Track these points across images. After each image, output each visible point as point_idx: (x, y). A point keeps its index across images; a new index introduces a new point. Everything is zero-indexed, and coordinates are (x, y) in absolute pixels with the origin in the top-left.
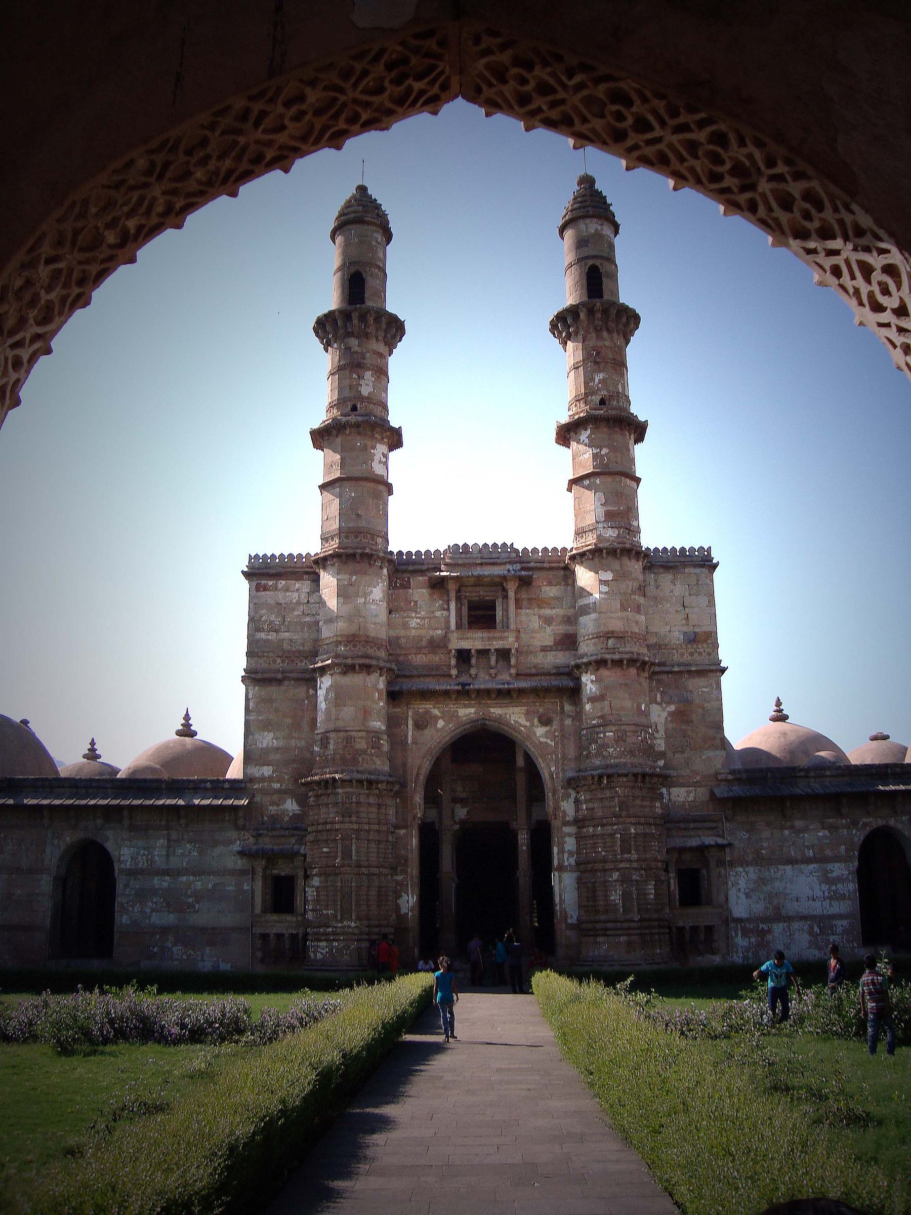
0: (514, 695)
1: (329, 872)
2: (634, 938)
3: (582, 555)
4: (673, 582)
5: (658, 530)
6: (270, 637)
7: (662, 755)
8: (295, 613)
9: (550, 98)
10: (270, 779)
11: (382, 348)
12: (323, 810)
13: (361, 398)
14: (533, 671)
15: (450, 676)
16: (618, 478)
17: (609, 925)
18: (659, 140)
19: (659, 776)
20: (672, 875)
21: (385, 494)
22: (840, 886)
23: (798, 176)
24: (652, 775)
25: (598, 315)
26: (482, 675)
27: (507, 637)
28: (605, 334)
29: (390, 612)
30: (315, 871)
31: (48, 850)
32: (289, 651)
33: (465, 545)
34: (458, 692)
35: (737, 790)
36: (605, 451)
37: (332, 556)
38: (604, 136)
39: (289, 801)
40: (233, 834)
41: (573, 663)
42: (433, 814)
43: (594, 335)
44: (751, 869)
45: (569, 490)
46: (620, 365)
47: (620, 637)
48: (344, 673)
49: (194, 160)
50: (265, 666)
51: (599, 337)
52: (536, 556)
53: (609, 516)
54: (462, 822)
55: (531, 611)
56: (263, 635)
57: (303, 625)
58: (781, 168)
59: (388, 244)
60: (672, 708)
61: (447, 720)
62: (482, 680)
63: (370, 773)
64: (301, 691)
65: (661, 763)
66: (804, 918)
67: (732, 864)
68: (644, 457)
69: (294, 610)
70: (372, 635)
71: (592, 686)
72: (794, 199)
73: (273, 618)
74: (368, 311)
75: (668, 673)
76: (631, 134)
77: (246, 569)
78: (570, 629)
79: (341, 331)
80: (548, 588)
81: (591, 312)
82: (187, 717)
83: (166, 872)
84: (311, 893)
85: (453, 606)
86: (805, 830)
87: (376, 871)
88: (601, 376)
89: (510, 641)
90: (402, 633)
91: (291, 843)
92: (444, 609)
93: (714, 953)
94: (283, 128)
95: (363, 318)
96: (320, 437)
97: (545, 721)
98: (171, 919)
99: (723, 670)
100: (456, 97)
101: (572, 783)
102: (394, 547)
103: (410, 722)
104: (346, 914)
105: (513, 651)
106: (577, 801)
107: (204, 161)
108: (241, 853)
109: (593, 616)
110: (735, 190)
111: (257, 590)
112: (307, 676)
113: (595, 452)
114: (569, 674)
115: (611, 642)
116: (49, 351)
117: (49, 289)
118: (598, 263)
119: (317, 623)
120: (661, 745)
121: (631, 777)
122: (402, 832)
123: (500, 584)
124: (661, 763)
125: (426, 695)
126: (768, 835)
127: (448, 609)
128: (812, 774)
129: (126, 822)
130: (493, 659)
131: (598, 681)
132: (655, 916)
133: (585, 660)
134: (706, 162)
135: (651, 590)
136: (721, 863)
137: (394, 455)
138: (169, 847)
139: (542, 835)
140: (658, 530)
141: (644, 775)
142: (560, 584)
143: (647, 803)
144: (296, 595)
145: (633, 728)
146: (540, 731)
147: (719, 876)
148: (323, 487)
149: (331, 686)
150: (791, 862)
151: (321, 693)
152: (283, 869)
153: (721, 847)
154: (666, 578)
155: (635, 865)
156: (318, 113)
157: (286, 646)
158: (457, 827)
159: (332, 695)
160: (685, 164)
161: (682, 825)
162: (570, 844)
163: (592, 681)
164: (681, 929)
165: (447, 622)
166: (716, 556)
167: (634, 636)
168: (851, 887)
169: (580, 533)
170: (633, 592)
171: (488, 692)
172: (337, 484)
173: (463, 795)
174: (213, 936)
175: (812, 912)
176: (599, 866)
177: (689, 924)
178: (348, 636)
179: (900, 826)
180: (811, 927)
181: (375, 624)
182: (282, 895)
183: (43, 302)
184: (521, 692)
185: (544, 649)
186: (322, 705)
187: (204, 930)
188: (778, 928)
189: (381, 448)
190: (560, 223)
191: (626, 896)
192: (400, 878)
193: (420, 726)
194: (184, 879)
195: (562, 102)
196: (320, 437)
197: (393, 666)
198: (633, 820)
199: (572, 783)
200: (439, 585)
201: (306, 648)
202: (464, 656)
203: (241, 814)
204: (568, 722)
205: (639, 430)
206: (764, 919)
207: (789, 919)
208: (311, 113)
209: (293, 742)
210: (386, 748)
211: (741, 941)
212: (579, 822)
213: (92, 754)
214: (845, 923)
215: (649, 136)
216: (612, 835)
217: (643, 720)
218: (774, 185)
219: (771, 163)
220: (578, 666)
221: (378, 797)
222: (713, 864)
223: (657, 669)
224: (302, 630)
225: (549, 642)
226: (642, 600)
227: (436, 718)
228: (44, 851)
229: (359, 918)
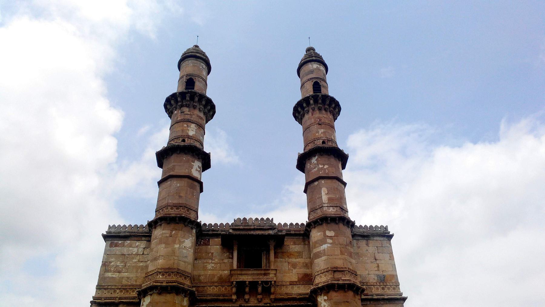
6: (114, 276)
8: (134, 261)
11: (202, 115)
13: (189, 137)
14: (286, 297)
15: (231, 301)
16: (335, 181)
21: (198, 188)
27: (269, 274)
28: (324, 112)
29: (196, 259)
32: (126, 286)
33: (245, 219)
36: (326, 167)
43: (318, 112)
45: (305, 191)
47: (341, 271)
48: (160, 294)
50: (108, 295)
51: (320, 113)
52: (286, 228)
53: (330, 200)
55: (284, 260)
56: (110, 275)
57: (137, 268)
59: (208, 74)
69: (133, 258)
71: (325, 304)
73: (118, 263)
74: (195, 93)
77: (105, 233)
78: (308, 271)
79: (179, 104)
80: (293, 246)
81: (316, 102)
88: (322, 130)
89: (271, 277)
90: (202, 273)
92: (230, 258)
95: (192, 98)
105: (273, 282)
109: (324, 258)
111: (111, 246)
113: (320, 166)
115: (338, 275)
127: (232, 258)
131: (329, 300)
133: (320, 286)
142: (300, 244)
144: (136, 249)
148: (160, 183)
149: (150, 302)
157: (124, 282)
163: (325, 300)
169: (311, 211)
172: (169, 180)
178: (165, 269)
181: (185, 262)
185: (292, 283)
189: (197, 164)
196: (162, 157)
197: (194, 289)
201: (138, 283)
202: (241, 285)
224: (137, 272)
225: (295, 279)
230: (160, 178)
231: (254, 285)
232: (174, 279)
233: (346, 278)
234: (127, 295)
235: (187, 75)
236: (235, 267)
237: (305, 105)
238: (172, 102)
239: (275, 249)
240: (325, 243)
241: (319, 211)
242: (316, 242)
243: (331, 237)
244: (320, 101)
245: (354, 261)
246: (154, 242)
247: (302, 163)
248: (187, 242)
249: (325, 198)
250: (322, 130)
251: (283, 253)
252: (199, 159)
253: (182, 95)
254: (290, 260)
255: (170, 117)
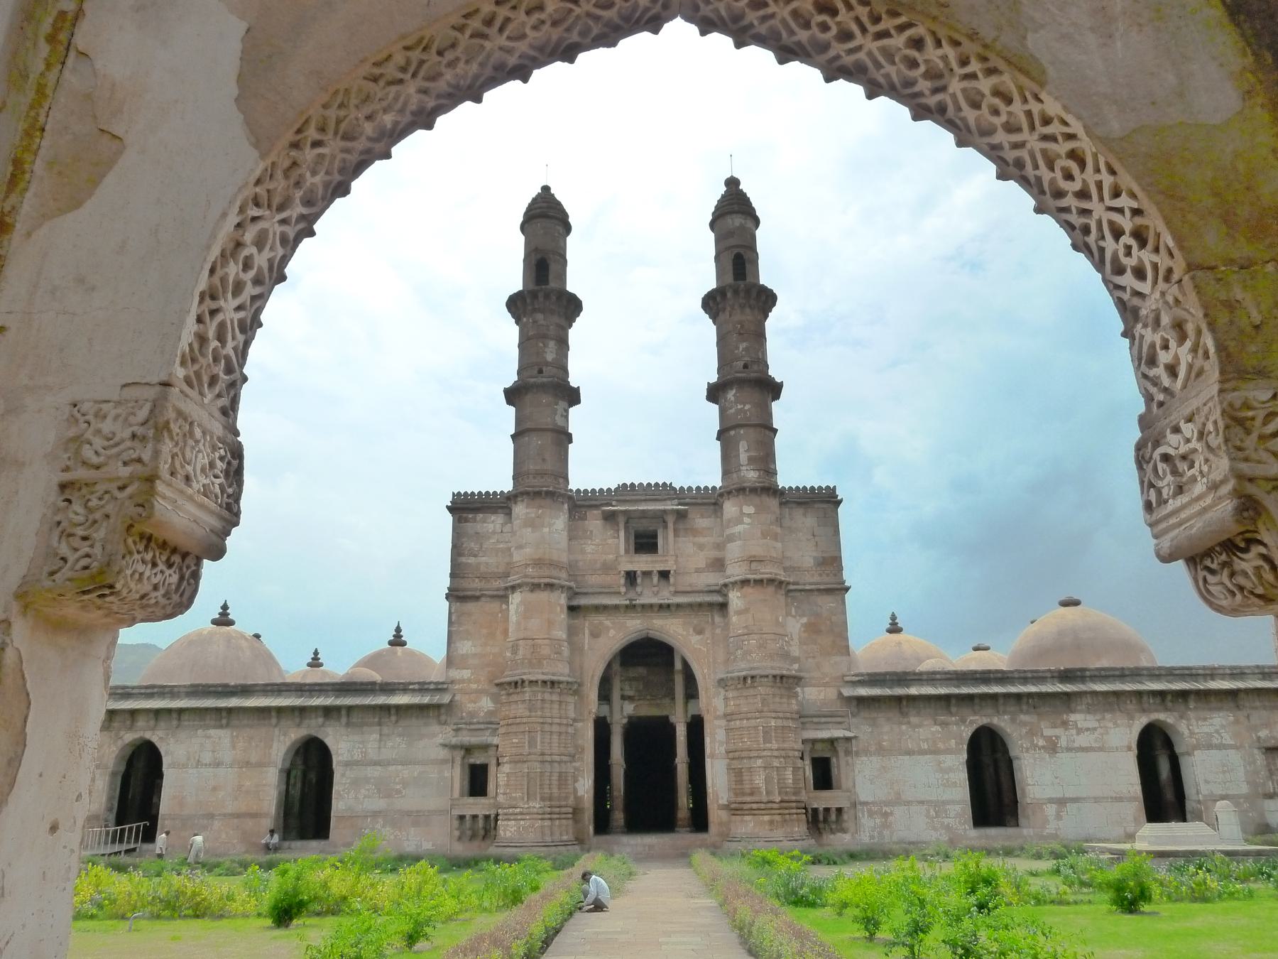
0: (673, 609)
1: (518, 760)
2: (777, 818)
3: (729, 493)
4: (805, 515)
5: (792, 472)
7: (796, 660)
9: (762, 13)
10: (469, 681)
11: (563, 322)
12: (513, 706)
13: (547, 364)
17: (755, 806)
18: (859, 48)
19: (795, 677)
20: (808, 762)
22: (952, 775)
23: (991, 72)
24: (788, 677)
25: (742, 294)
26: (646, 592)
28: (748, 310)
30: (506, 759)
31: (275, 745)
33: (632, 484)
34: (627, 606)
35: (863, 691)
36: (747, 407)
37: (522, 494)
38: (809, 49)
39: (485, 699)
40: (435, 728)
41: (721, 582)
42: (605, 710)
44: (874, 759)
45: (718, 439)
46: (760, 336)
48: (532, 591)
49: (445, 61)
53: (751, 460)
54: (630, 717)
58: (975, 66)
60: (805, 620)
61: (618, 632)
62: (647, 596)
63: (553, 674)
64: (494, 606)
65: (796, 666)
66: (922, 802)
67: (857, 754)
68: (779, 410)
69: (489, 538)
70: (555, 558)
72: (983, 95)
75: (801, 591)
76: (834, 44)
78: (717, 554)
81: (736, 292)
82: (398, 630)
83: (375, 763)
84: (502, 779)
85: (622, 534)
86: (920, 726)
87: (557, 758)
88: (744, 345)
89: (669, 566)
91: (486, 738)
93: (844, 831)
94: (523, 36)
95: (547, 296)
96: (512, 395)
97: (700, 632)
98: (380, 804)
99: (847, 589)
100: (674, 17)
101: (722, 683)
102: (573, 486)
103: (587, 631)
104: (530, 796)
106: (726, 699)
107: (451, 64)
108: (445, 746)
109: (738, 543)
110: (927, 92)
112: (501, 593)
114: (718, 592)
115: (754, 565)
116: (311, 233)
117: (314, 173)
118: (742, 251)
119: (509, 549)
120: (795, 651)
121: (771, 678)
122: (579, 725)
123: (661, 517)
124: (796, 666)
125: (599, 609)
126: (887, 728)
128: (925, 677)
129: (344, 720)
130: (655, 579)
131: (744, 596)
132: (794, 798)
133: (732, 580)
134: (902, 67)
135: (787, 522)
136: (848, 753)
137: (571, 410)
138: (380, 740)
139: (696, 728)
140: (792, 472)
141: (782, 677)
143: (785, 700)
145: (773, 637)
146: (695, 639)
147: (847, 764)
150: (909, 753)
151: (512, 608)
152: (478, 759)
153: (848, 739)
154: (798, 513)
155: (776, 753)
156: (555, 24)
157: (483, 568)
158: (625, 721)
159: (522, 609)
160: (882, 71)
161: (815, 720)
162: (721, 735)
164: (815, 811)
165: (618, 546)
166: (840, 494)
167: (772, 561)
168: (962, 776)
169: (726, 473)
170: (771, 523)
171: (651, 606)
173: (631, 693)
174: (418, 818)
175: (928, 798)
176: (744, 754)
177: (821, 806)
179: (1002, 724)
180: (928, 811)
182: (477, 782)
183: (308, 184)
184: (678, 606)
185: (698, 571)
186: (513, 617)
187: (409, 813)
188: (898, 811)
189: (562, 404)
190: (710, 218)
191: (768, 780)
192: (577, 764)
193: (595, 635)
194: (392, 768)
195: (773, 16)
196: (512, 395)
197: (572, 584)
198: (774, 715)
199: (722, 683)
200: (610, 517)
202: (631, 577)
203: (443, 711)
204: (718, 631)
205: (775, 390)
206: (887, 803)
207: (908, 803)
208: (548, 23)
209: (488, 649)
210: (566, 651)
211: (867, 822)
212: (728, 717)
213: (315, 662)
214: (958, 808)
215: (851, 45)
216: (756, 728)
217: (781, 631)
218: (965, 84)
219: (964, 62)
220: (726, 585)
221: (560, 694)
222: (841, 754)
223: (792, 587)
226: (779, 530)
227: (608, 629)
228: (271, 747)
229: (543, 799)
230: (513, 432)
231: (647, 574)
232: (546, 574)
233: (767, 571)
234: (488, 586)
235: (536, 250)
236: (622, 551)
237: (718, 299)
238: (519, 303)
239: (675, 523)
240: (742, 522)
241: (735, 475)
242: (729, 521)
243: (749, 515)
244: (742, 294)
245: (779, 545)
246: (516, 523)
247: (714, 393)
248: (559, 522)
249: (743, 457)
250: (744, 345)
251: (686, 529)
252: (563, 399)
253: (534, 295)
254: (696, 539)
255: (517, 323)
